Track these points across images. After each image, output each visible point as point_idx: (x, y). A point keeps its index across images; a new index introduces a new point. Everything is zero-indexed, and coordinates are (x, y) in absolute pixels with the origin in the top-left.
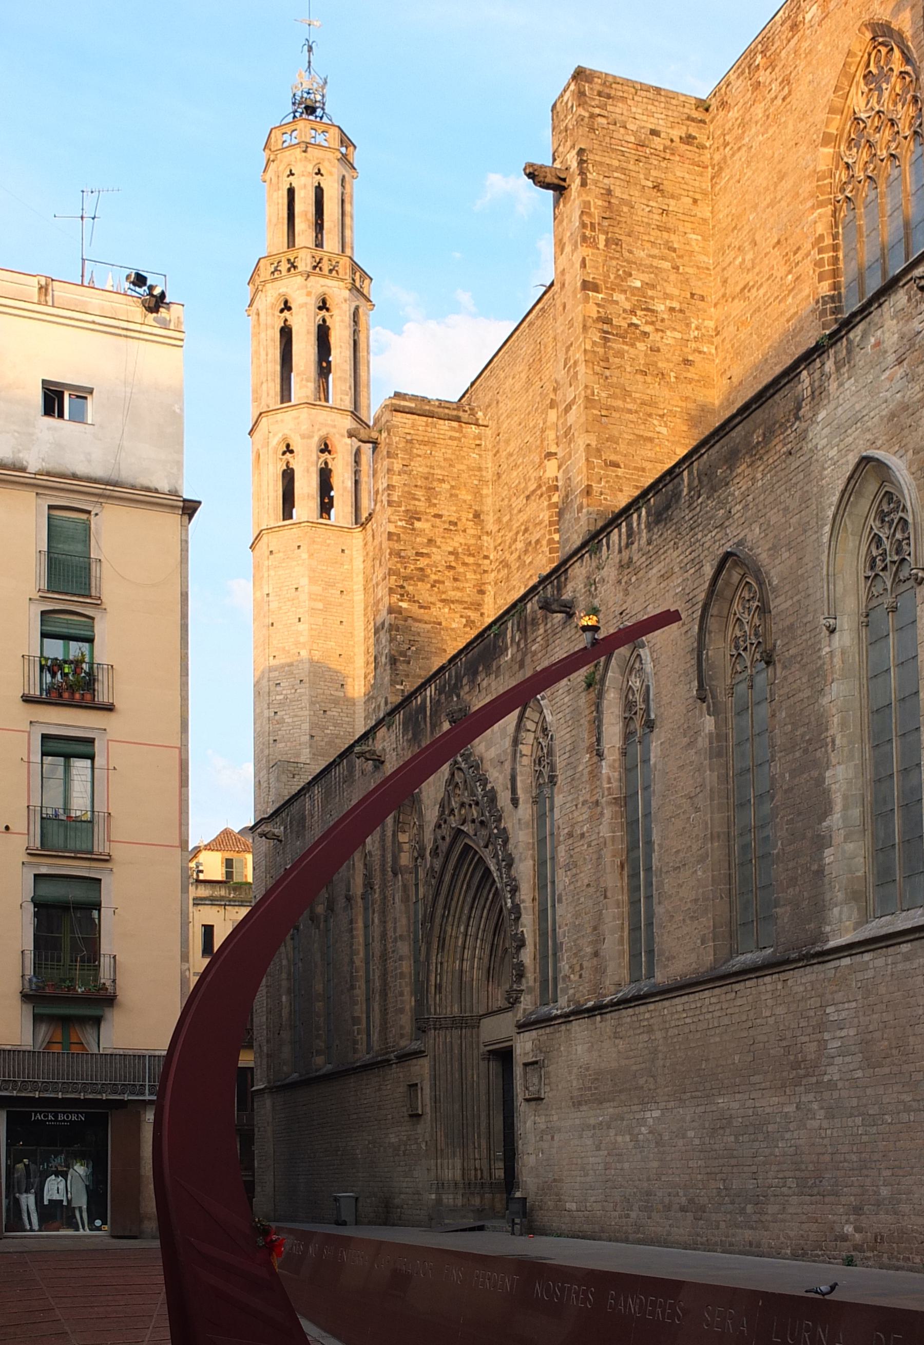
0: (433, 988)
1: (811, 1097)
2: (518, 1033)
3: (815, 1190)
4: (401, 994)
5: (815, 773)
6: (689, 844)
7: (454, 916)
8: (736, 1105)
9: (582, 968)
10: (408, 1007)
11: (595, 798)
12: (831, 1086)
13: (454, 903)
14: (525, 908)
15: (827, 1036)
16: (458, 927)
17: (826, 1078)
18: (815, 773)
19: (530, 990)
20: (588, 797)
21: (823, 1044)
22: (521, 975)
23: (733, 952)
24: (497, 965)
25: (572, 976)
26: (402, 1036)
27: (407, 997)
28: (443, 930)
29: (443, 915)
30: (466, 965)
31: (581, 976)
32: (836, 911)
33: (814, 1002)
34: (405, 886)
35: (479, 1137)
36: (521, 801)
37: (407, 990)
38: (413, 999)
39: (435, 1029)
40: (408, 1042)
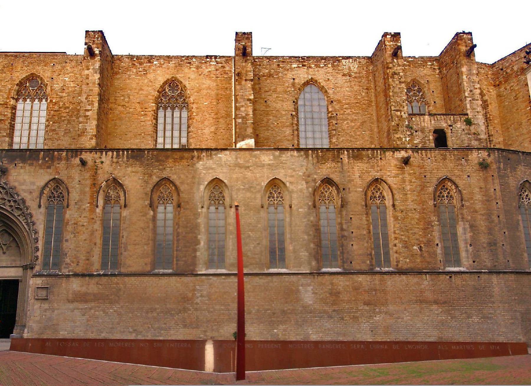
1: (189, 306)
3: (190, 327)
5: (194, 235)
6: (141, 239)
8: (158, 306)
9: (78, 262)
11: (92, 217)
12: (197, 304)
15: (196, 292)
17: (195, 302)
18: (194, 235)
19: (39, 265)
20: (88, 216)
21: (194, 294)
23: (154, 269)
25: (72, 264)
31: (77, 265)
32: (201, 266)
33: (192, 284)
36: (42, 207)
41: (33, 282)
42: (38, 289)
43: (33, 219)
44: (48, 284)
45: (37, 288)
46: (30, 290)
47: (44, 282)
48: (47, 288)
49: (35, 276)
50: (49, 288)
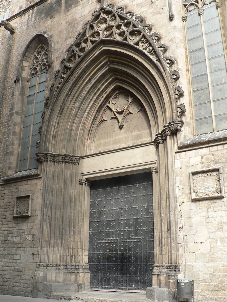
0: (52, 136)
2: (176, 153)
4: (13, 144)
7: (74, 96)
10: (16, 152)
13: (75, 89)
14: (182, 74)
16: (74, 103)
19: (188, 124)
22: (183, 113)
24: (94, 130)
26: (10, 168)
27: (16, 146)
28: (64, 103)
29: (67, 95)
30: (74, 127)
34: (23, 88)
35: (74, 234)
37: (16, 142)
38: (20, 147)
39: (50, 161)
40: (14, 172)
41: (182, 162)
42: (196, 176)
43: (162, 42)
44: (216, 163)
45: (194, 174)
46: (177, 181)
47: (207, 159)
48: (217, 170)
49: (183, 148)
50: (221, 171)
